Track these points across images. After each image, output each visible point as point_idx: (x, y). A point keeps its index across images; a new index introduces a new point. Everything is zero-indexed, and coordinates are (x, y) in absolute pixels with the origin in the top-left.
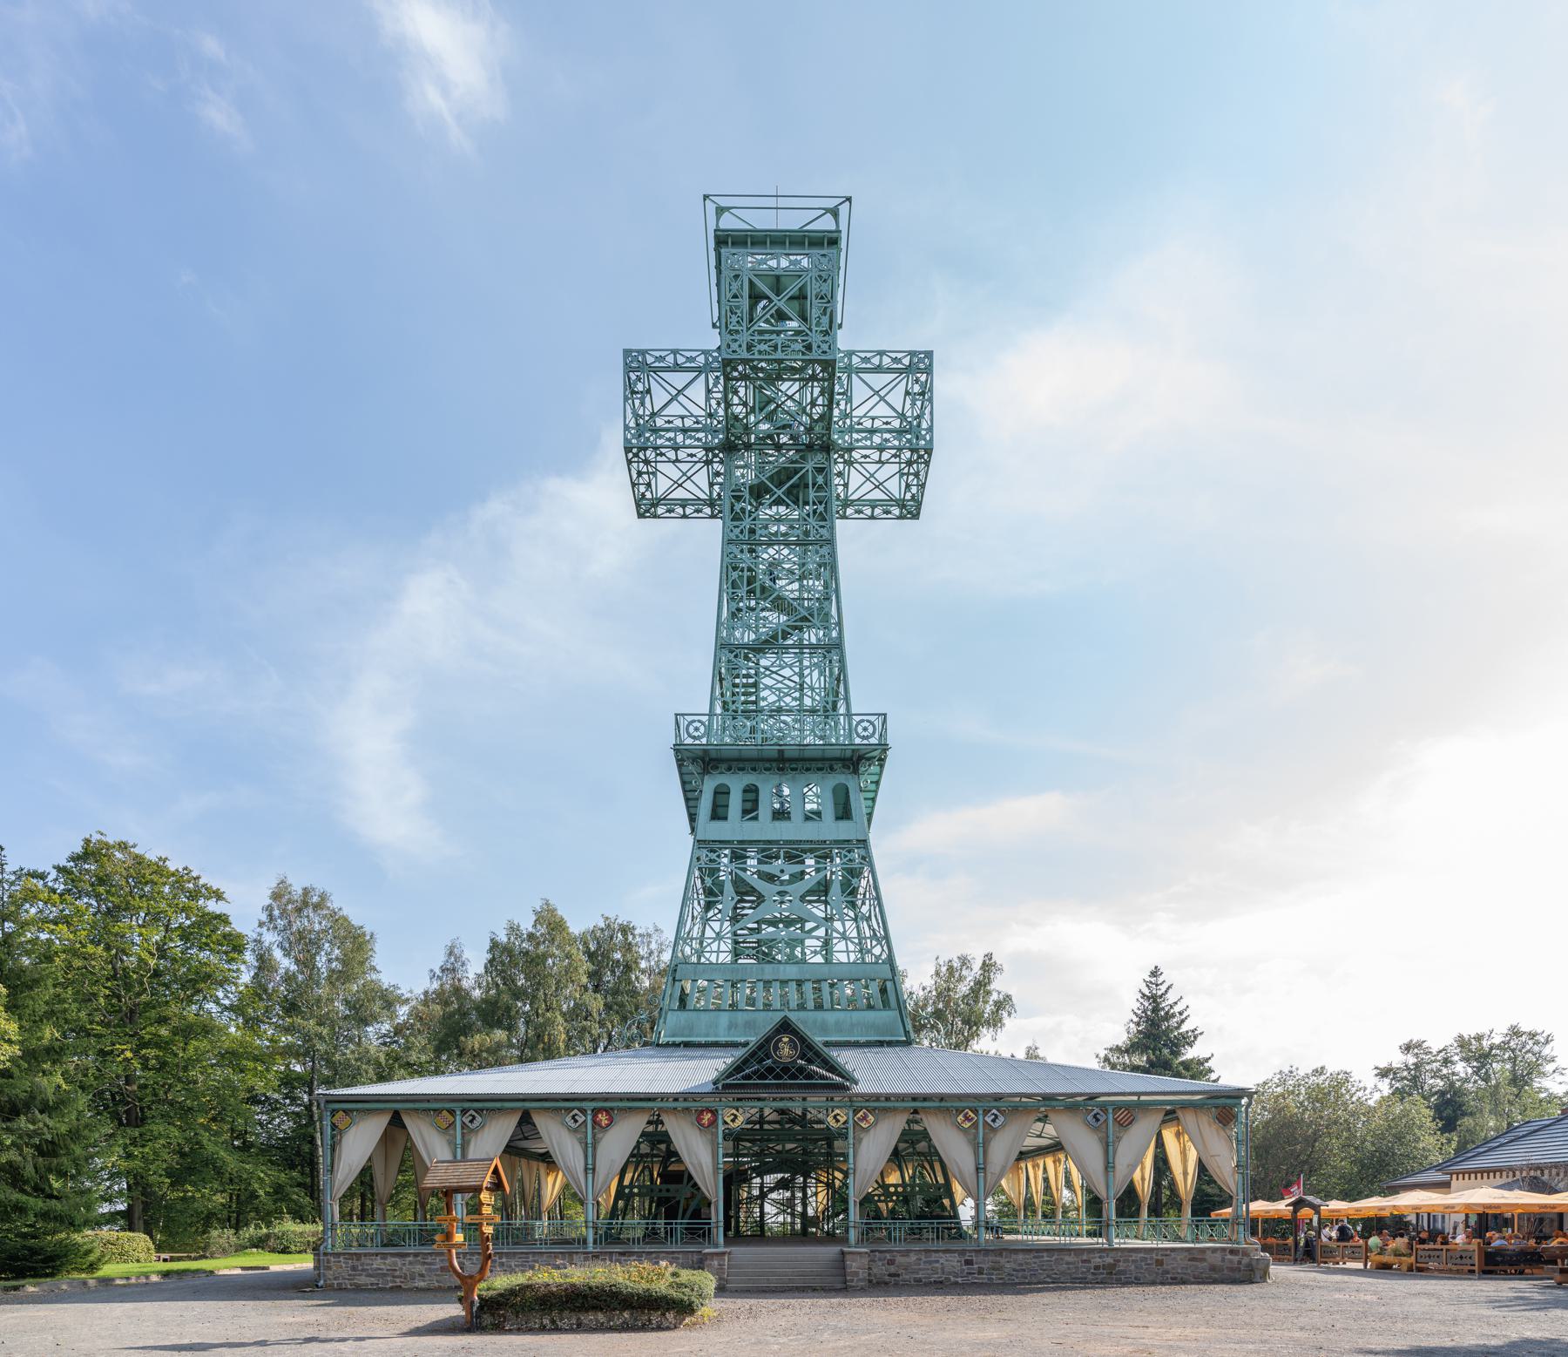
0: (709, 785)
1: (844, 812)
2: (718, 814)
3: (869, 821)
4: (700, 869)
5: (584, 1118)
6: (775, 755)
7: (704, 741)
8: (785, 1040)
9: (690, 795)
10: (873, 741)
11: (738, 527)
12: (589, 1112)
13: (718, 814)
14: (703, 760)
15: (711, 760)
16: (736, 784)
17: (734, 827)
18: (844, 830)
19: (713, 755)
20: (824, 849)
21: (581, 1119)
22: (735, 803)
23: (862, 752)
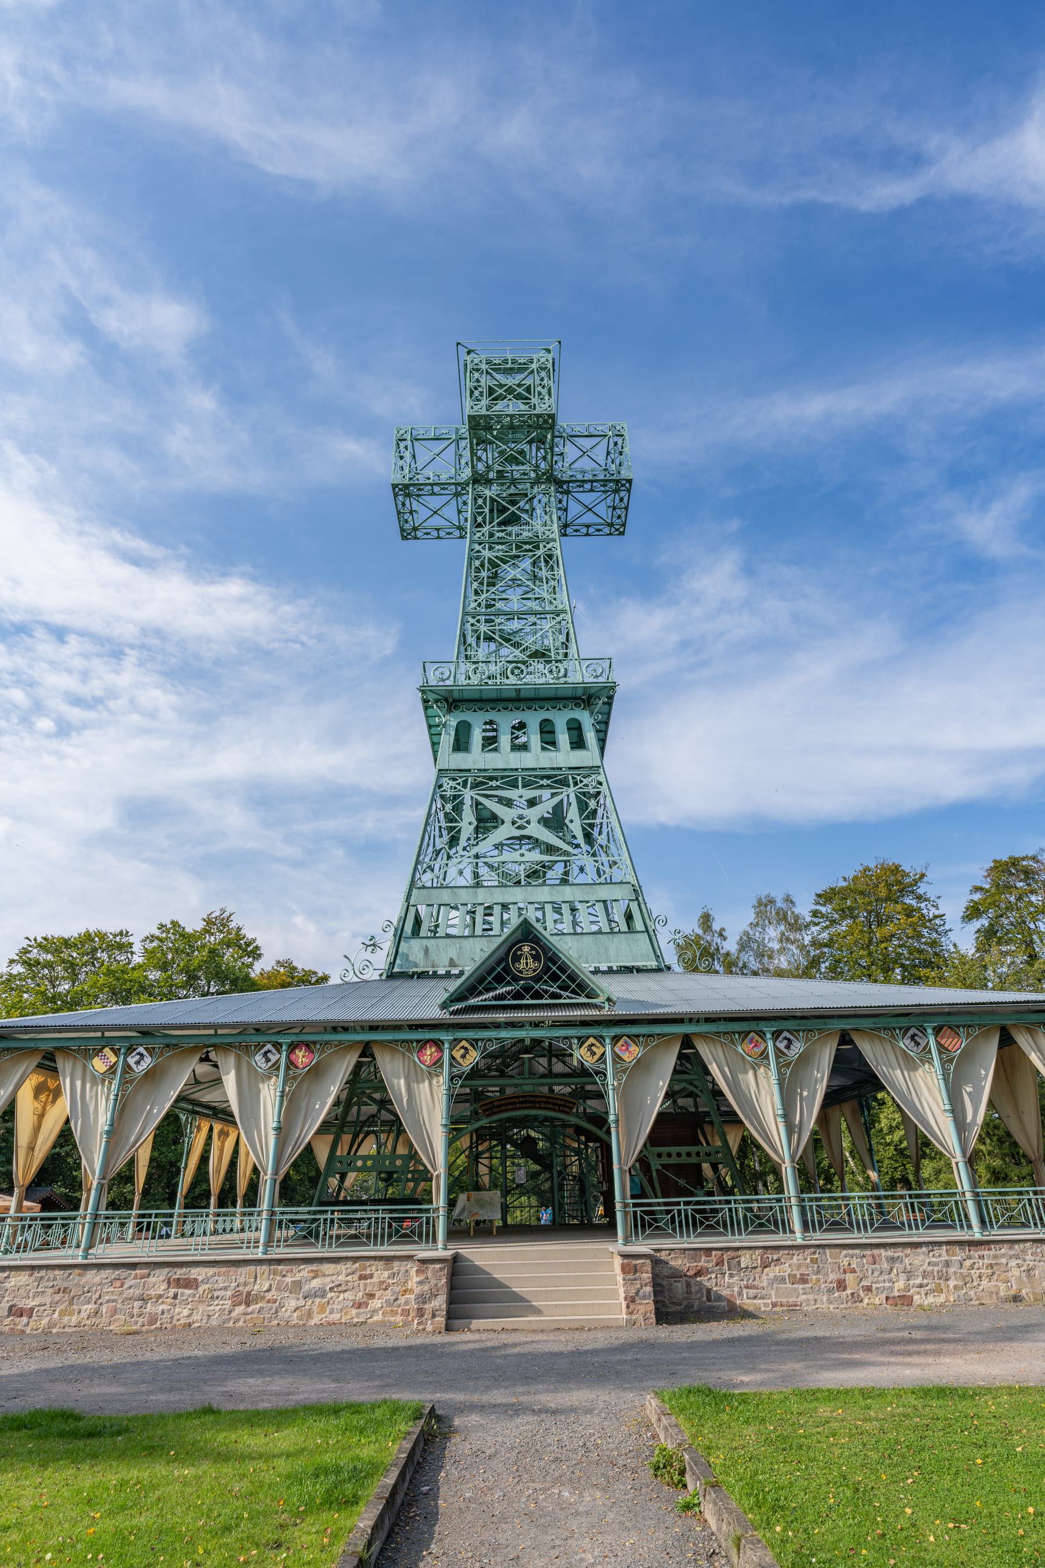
0: (453, 721)
1: (578, 743)
2: (461, 744)
3: (602, 750)
4: (442, 797)
5: (278, 1056)
6: (513, 695)
7: (448, 683)
8: (526, 949)
9: (434, 730)
10: (601, 679)
11: (480, 531)
12: (284, 1047)
13: (461, 744)
14: (446, 700)
15: (454, 701)
16: (478, 722)
17: (476, 758)
18: (579, 758)
19: (456, 695)
20: (561, 775)
21: (273, 1058)
22: (477, 736)
23: (592, 691)
